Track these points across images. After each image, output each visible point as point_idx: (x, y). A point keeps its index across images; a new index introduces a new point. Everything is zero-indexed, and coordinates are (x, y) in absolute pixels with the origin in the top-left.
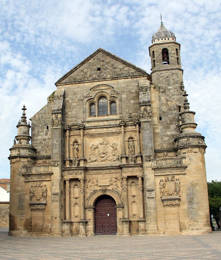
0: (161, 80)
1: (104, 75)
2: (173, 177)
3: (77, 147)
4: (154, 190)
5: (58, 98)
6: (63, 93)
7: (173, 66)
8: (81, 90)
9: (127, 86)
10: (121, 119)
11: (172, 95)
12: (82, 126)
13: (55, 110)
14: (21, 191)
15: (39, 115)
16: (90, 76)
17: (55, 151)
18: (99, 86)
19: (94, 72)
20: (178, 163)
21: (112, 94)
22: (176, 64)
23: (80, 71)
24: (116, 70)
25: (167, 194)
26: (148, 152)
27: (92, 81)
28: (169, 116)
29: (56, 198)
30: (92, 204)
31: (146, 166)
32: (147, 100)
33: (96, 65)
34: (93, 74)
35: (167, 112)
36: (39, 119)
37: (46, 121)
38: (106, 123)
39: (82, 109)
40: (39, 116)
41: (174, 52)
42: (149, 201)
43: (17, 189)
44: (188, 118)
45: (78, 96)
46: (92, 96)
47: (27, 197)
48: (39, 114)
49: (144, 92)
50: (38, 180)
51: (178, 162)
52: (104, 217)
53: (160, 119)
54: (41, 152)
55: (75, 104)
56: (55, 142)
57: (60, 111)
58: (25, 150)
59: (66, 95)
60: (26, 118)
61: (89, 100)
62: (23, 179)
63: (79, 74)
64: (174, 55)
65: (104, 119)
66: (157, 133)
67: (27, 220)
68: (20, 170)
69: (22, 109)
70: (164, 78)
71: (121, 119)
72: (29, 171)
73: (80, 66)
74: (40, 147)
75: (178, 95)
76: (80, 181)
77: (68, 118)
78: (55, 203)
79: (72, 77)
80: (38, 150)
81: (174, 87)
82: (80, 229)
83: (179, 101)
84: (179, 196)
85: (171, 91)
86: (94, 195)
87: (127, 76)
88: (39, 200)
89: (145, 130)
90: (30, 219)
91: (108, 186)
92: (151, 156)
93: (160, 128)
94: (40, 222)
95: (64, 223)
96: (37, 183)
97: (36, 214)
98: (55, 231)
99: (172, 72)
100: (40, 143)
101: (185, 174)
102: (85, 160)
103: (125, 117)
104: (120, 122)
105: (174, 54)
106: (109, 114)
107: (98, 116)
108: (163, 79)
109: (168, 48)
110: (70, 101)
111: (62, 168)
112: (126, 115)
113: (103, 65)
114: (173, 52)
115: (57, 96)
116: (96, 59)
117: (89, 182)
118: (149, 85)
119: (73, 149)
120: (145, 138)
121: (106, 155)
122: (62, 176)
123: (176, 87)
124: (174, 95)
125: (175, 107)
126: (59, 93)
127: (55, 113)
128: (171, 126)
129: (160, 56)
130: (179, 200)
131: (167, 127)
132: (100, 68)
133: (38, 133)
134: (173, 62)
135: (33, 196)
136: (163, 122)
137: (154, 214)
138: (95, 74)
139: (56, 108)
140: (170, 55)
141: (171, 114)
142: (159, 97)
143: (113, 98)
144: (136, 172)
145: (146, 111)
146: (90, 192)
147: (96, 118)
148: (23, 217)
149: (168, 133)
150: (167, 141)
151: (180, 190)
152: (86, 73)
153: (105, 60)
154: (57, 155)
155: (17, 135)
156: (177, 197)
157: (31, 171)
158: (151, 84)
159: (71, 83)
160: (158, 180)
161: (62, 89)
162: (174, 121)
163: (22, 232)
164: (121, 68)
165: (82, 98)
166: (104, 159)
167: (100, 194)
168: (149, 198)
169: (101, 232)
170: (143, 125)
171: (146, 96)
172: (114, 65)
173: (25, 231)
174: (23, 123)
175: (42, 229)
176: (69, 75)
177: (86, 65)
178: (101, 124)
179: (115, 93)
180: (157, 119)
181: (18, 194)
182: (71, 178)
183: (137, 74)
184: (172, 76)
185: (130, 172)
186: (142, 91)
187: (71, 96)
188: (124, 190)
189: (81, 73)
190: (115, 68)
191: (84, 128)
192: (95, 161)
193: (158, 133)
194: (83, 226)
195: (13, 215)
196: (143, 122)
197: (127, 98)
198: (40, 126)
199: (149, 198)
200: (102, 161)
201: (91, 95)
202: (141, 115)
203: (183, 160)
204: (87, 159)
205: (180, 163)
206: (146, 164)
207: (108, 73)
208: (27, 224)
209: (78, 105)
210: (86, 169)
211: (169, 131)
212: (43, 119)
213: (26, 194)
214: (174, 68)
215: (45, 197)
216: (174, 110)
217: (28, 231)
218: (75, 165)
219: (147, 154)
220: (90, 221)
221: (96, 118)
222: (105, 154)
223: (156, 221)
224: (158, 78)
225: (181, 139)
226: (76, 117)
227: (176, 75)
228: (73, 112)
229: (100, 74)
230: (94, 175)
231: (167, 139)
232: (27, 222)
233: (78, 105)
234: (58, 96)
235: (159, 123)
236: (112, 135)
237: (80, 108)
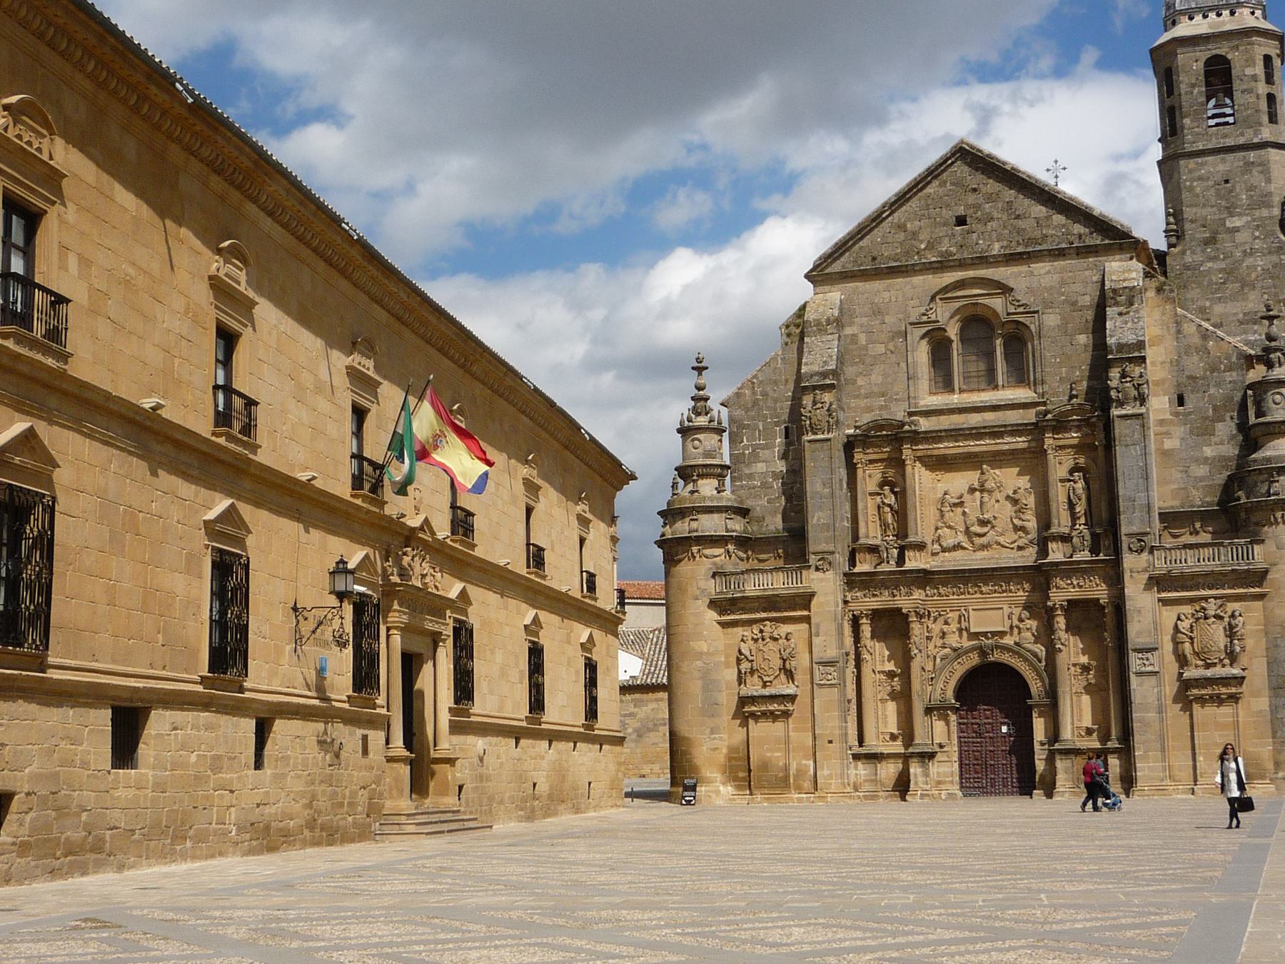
0: (1198, 190)
1: (981, 242)
2: (1221, 606)
3: (891, 499)
4: (1157, 649)
5: (818, 330)
6: (836, 313)
7: (1250, 131)
8: (900, 299)
9: (1063, 283)
10: (1044, 404)
11: (1245, 251)
12: (907, 428)
13: (812, 376)
14: (707, 654)
15: (753, 388)
16: (930, 246)
17: (818, 520)
18: (961, 284)
19: (944, 234)
20: (1240, 558)
21: (1009, 314)
22: (1260, 124)
23: (891, 227)
24: (1021, 224)
25: (1200, 663)
26: (1137, 521)
27: (937, 265)
28: (1212, 391)
29: (830, 677)
30: (950, 694)
31: (1131, 566)
32: (1130, 338)
33: (948, 205)
34: (939, 241)
35: (1204, 378)
36: (755, 403)
37: (782, 408)
38: (990, 418)
39: (905, 368)
40: (754, 393)
41: (1253, 73)
42: (1141, 684)
43: (696, 648)
44: (1277, 401)
45: (888, 319)
46: (938, 322)
47: (732, 674)
48: (753, 383)
49: (1122, 309)
50: (764, 615)
51: (1240, 554)
52: (991, 735)
53: (1181, 401)
54: (768, 520)
55: (881, 349)
56: (819, 487)
57: (831, 377)
58: (716, 516)
59: (845, 319)
60: (706, 399)
61: (928, 332)
62: (712, 615)
63: (889, 240)
64: (1253, 84)
65: (982, 402)
66: (1168, 450)
67: (732, 749)
68: (702, 584)
69: (693, 368)
70: (1211, 183)
71: (1044, 404)
72: (732, 587)
73: (893, 208)
74: (764, 502)
75: (1270, 253)
76: (907, 616)
77: (857, 397)
78: (826, 691)
79: (867, 250)
80: (757, 512)
81: (1254, 220)
82: (912, 777)
83: (1270, 277)
84: (1243, 670)
85: (1241, 237)
86: (956, 663)
87: (1064, 246)
88: (771, 682)
89: (1126, 446)
90: (741, 747)
91: (1002, 634)
92: (1146, 534)
93: (1178, 434)
94: (776, 754)
95: (859, 759)
96: (762, 627)
97: (759, 729)
98: (831, 784)
99: (1244, 157)
100: (765, 485)
101: (1261, 597)
102: (921, 547)
103: (1056, 394)
104: (1037, 415)
105: (1254, 78)
106: (1000, 383)
107: (961, 391)
108: (1207, 189)
109: (1229, 57)
110: (863, 339)
111: (845, 575)
112: (1058, 387)
113: (977, 207)
114: (1249, 71)
115: (815, 320)
116: (948, 184)
117: (935, 621)
118: (1141, 284)
119: (879, 510)
120: (1127, 473)
121: (993, 527)
122: (846, 602)
123: (1261, 218)
124: (1251, 254)
125: (1234, 359)
126: (821, 310)
127: (814, 388)
128: (1219, 426)
129: (1196, 91)
130: (1240, 680)
131: (1204, 431)
132: (966, 216)
133: (753, 451)
134: (1248, 116)
135: (752, 668)
136: (1190, 413)
137: (1156, 726)
138: (946, 241)
139: (816, 368)
140: (1237, 85)
141: (1218, 385)
142: (1177, 323)
143: (1014, 326)
144: (1099, 590)
145: (1128, 379)
146: (941, 653)
147: (955, 399)
148: (721, 739)
149: (1208, 452)
150: (1202, 479)
151: (1243, 649)
152: (914, 235)
153: (981, 186)
154: (828, 531)
155: (679, 462)
156: (1236, 671)
157: (741, 586)
158: (1147, 277)
159: (864, 275)
160: (1169, 615)
161: (835, 295)
162: (1228, 411)
163: (719, 791)
164: (1041, 215)
165: (904, 328)
166: (984, 540)
167: (974, 660)
168: (1140, 674)
169: (983, 787)
170: (1120, 429)
171: (1129, 325)
172: (1015, 205)
173: (729, 788)
174: (702, 421)
175: (787, 777)
176: (854, 244)
177: (914, 204)
178: (975, 419)
179: (1021, 310)
180: (1170, 402)
181: (699, 663)
182: (876, 606)
183: (1097, 240)
184: (1243, 174)
185: (1074, 587)
186: (1117, 304)
187: (864, 320)
188: (1057, 646)
189: (897, 236)
190: (1019, 215)
191: (916, 437)
192: (954, 546)
193: (1172, 450)
194: (923, 767)
195: (687, 735)
196: (1120, 417)
197: (1063, 327)
198: (761, 428)
199: (1140, 674)
200: (984, 547)
201: (933, 318)
202: (1113, 394)
203: (1255, 546)
204: (928, 540)
205: (1245, 558)
206: (1129, 561)
207: (994, 235)
208: (734, 762)
209: (892, 352)
210: (924, 578)
211: (1210, 445)
212: (770, 403)
213: (727, 665)
214: (1256, 140)
215: (790, 675)
216: (1230, 370)
217: (738, 788)
218: (888, 562)
219: (1135, 529)
220: (945, 749)
221: (956, 396)
222: (989, 525)
223: (1163, 750)
224: (1188, 183)
225: (1249, 475)
226: (883, 396)
227: (1260, 168)
228: (873, 377)
229: (964, 238)
230: (951, 597)
231: (1202, 471)
232: (734, 758)
233: (892, 352)
234: (818, 323)
235: (1177, 414)
236: (1011, 457)
237: (899, 364)
